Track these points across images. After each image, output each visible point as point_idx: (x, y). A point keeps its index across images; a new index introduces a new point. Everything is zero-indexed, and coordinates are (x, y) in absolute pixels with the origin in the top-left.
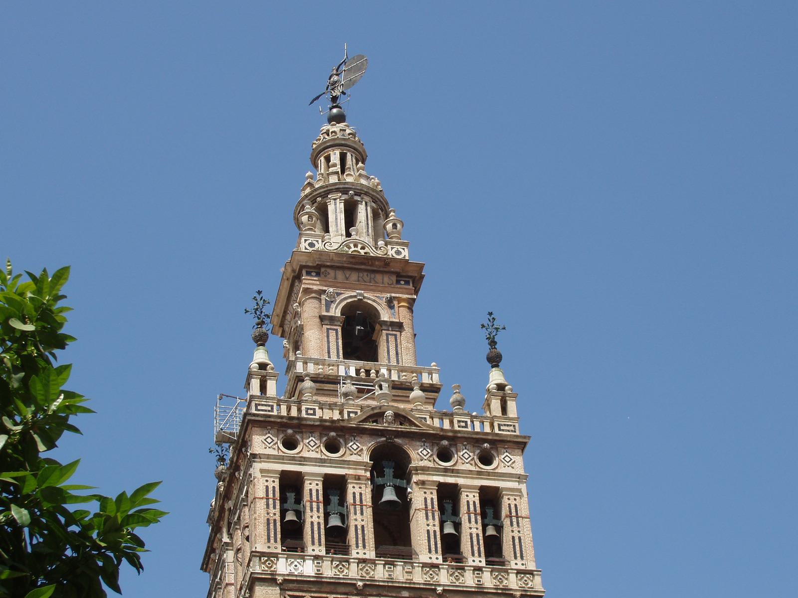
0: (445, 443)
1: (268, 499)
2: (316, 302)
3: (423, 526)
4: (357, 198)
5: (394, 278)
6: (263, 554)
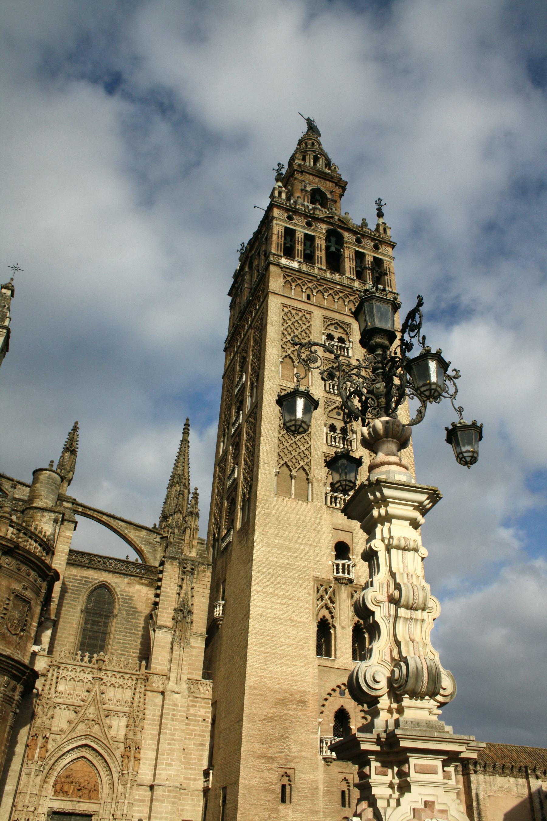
0: (359, 236)
1: (278, 235)
2: (300, 184)
3: (349, 265)
4: (319, 156)
5: (334, 185)
6: (274, 254)
